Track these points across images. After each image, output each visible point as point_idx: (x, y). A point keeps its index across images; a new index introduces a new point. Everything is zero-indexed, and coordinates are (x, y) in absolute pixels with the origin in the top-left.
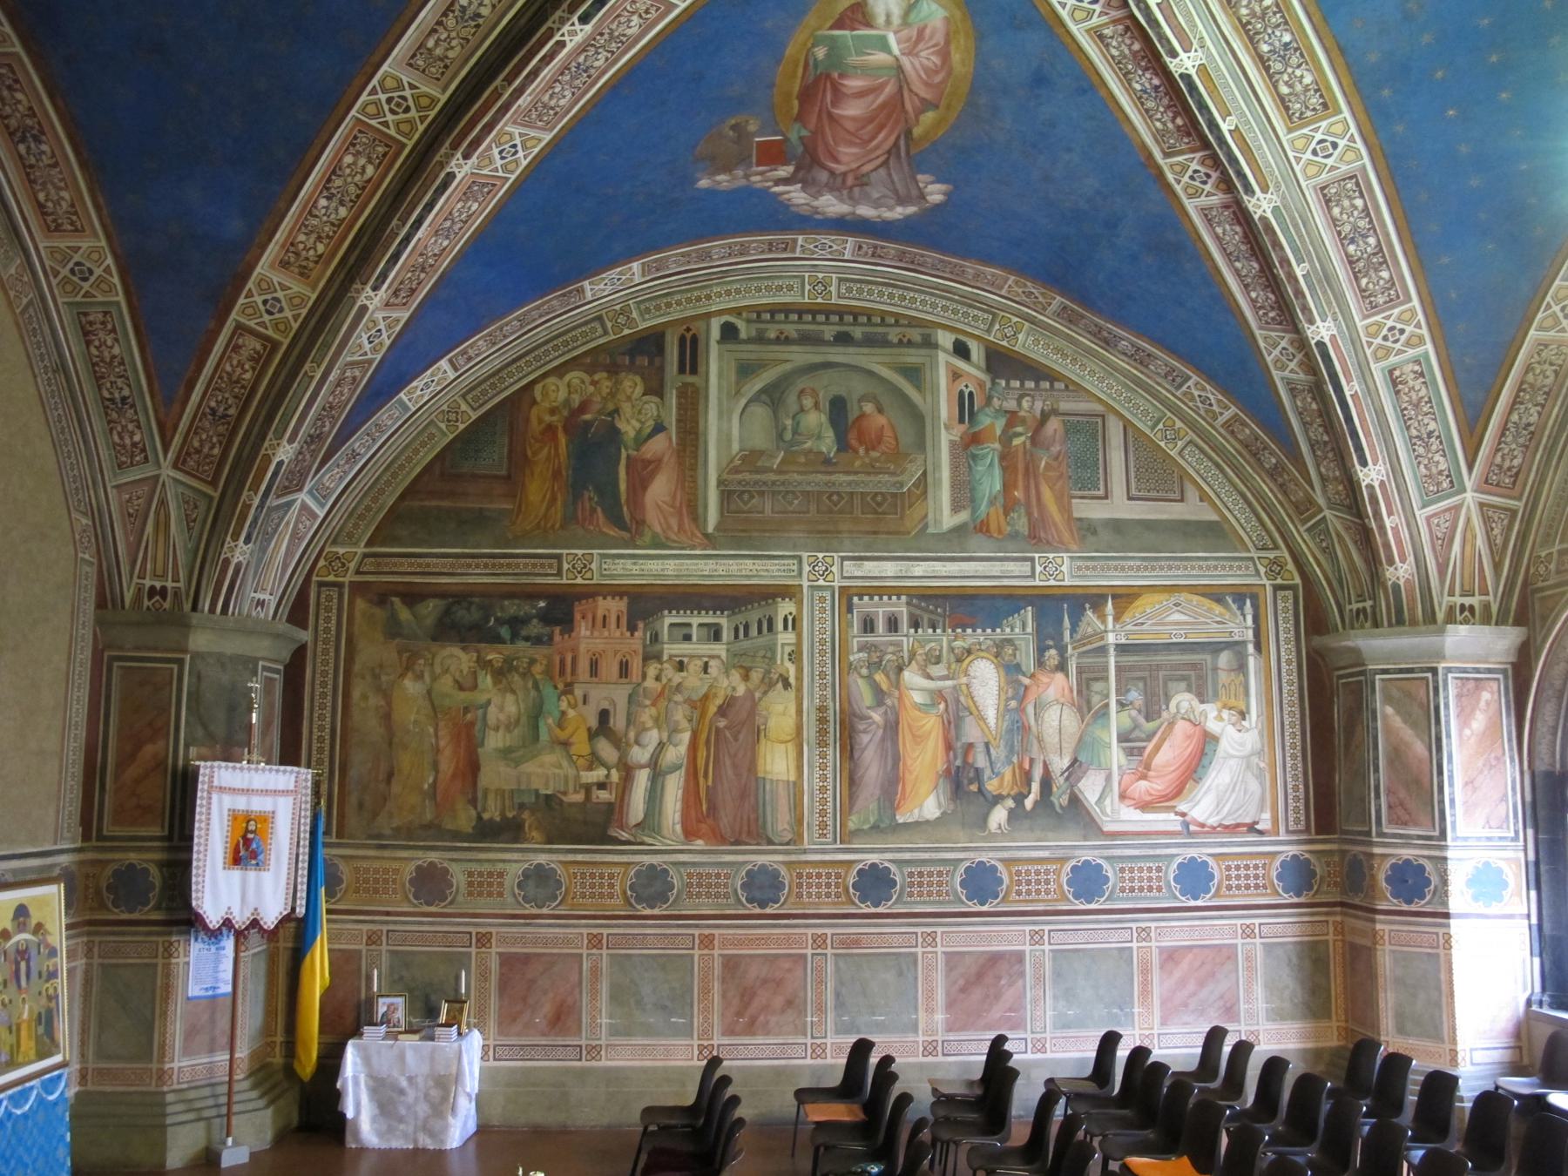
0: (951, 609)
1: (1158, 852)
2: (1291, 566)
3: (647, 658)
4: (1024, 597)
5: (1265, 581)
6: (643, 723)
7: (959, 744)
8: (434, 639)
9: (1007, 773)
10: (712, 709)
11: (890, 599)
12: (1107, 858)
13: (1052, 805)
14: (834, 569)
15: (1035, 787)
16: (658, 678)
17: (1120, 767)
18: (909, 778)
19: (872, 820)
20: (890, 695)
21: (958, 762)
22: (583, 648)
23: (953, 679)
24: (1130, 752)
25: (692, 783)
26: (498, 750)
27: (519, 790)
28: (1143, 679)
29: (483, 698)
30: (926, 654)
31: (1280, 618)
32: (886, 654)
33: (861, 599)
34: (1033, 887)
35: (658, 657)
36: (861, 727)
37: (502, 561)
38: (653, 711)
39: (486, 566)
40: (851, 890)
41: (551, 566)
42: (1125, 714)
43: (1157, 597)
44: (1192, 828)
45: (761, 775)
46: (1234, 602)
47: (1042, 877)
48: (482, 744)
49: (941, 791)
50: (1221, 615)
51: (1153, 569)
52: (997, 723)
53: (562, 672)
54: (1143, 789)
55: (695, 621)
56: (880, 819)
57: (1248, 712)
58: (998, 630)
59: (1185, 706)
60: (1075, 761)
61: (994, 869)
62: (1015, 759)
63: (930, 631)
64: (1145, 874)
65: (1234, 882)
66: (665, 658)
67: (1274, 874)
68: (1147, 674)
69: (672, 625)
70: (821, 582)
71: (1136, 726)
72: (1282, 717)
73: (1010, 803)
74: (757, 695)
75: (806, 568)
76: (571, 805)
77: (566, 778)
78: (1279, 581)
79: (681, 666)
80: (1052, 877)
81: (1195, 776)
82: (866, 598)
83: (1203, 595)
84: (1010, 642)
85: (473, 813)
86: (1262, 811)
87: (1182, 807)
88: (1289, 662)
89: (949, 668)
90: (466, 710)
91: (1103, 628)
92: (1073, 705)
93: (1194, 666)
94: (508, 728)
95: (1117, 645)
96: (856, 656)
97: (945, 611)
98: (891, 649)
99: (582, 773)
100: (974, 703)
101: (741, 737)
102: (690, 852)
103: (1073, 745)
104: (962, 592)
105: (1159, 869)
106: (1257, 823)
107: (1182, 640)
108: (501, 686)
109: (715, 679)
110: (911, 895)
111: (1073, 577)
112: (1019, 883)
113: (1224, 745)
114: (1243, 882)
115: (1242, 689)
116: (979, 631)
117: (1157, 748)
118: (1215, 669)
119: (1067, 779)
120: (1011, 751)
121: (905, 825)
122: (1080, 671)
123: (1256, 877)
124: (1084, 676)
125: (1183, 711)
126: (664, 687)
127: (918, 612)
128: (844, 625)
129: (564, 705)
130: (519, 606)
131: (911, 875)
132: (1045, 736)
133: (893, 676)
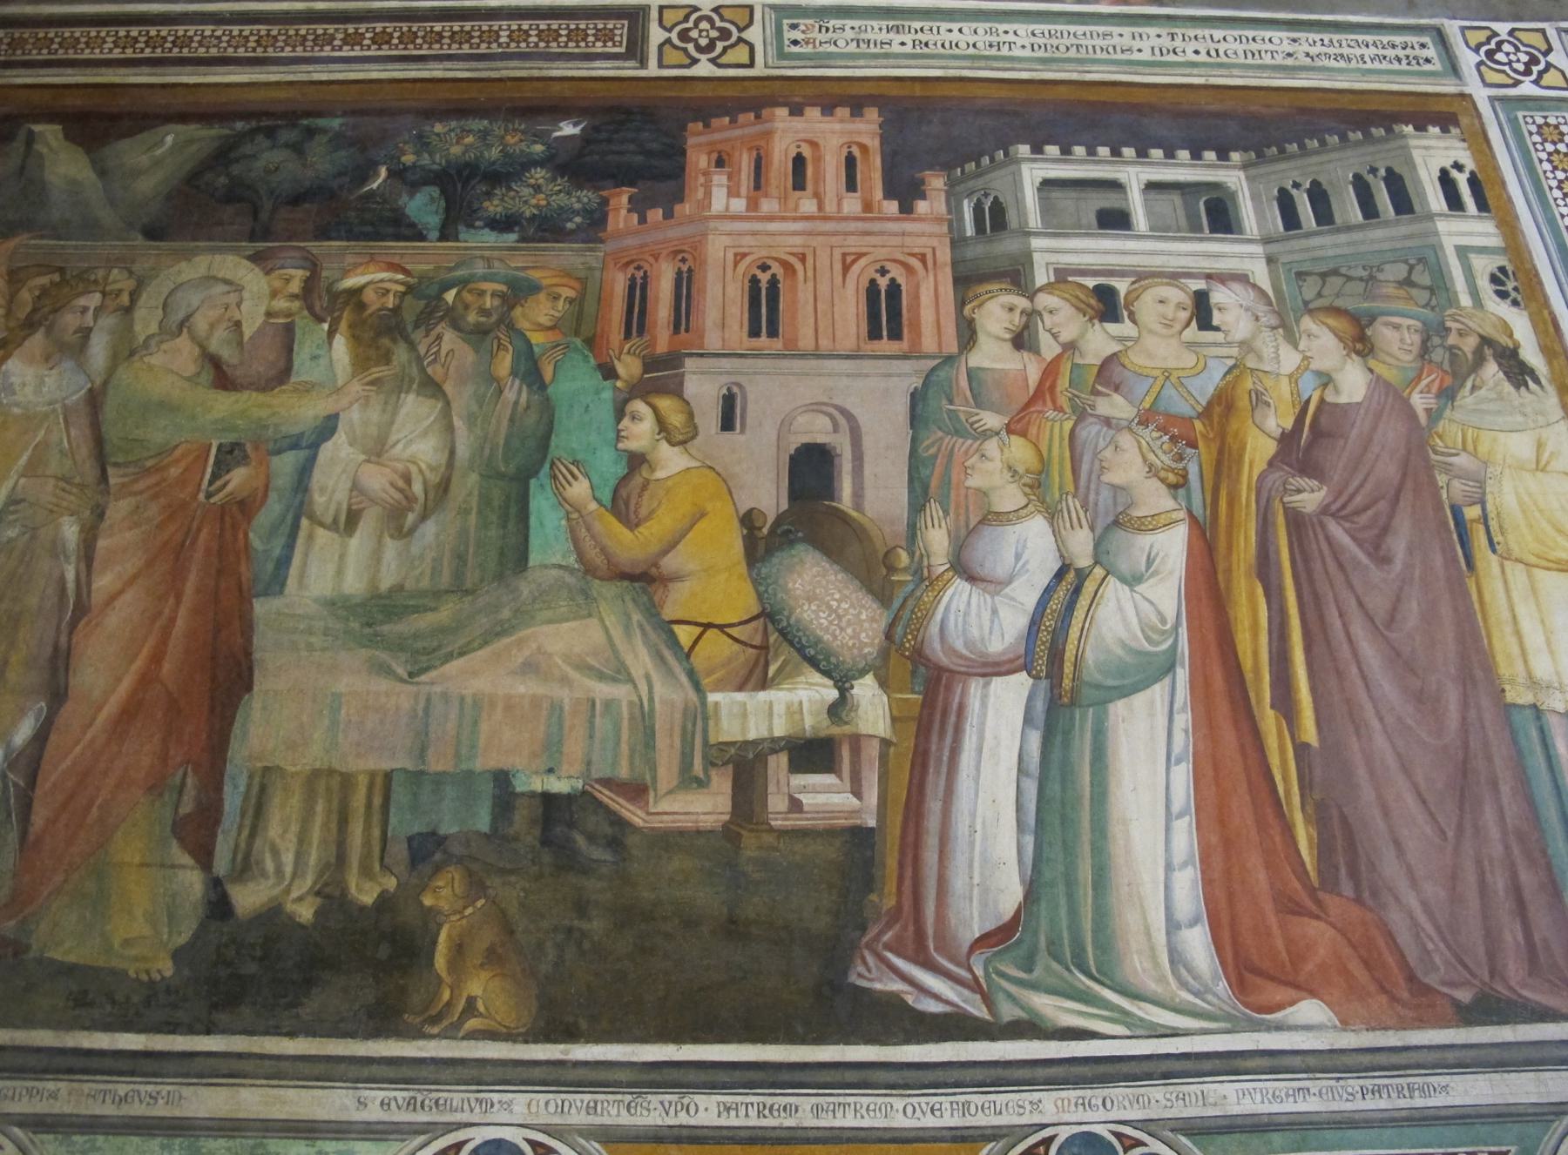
3: (967, 280)
6: (983, 494)
8: (153, 233)
10: (1259, 448)
16: (1022, 340)
22: (717, 248)
25: (1229, 736)
26: (337, 605)
27: (417, 777)
29: (306, 412)
35: (1016, 275)
37: (438, 27)
38: (1019, 450)
39: (381, 39)
41: (607, 36)
45: (1517, 695)
48: (277, 583)
53: (637, 318)
55: (1134, 175)
66: (1041, 277)
69: (1047, 184)
74: (1419, 402)
75: (1468, 59)
76: (668, 841)
77: (644, 723)
79: (1106, 305)
85: (192, 882)
90: (231, 455)
94: (397, 521)
99: (713, 697)
101: (1398, 545)
102: (1274, 1063)
108: (377, 372)
109: (1246, 346)
126: (1050, 371)
129: (640, 431)
130: (484, 135)
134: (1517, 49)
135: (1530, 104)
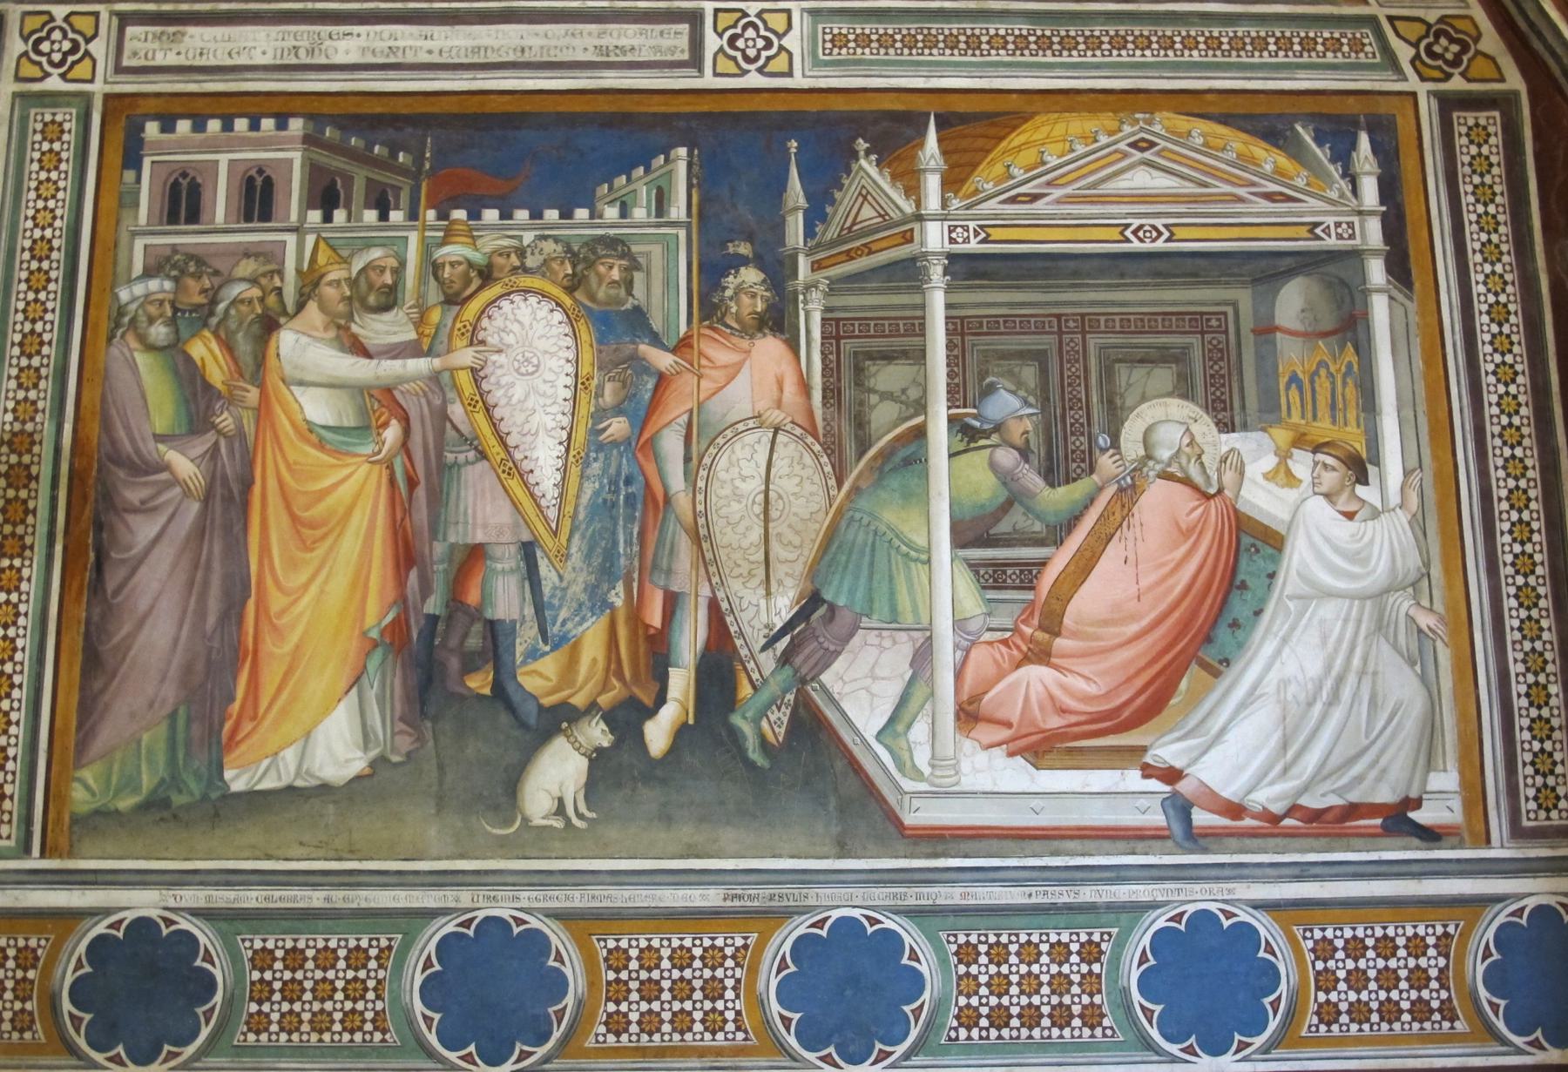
0: (439, 153)
1: (1088, 894)
2: (1491, 41)
4: (666, 120)
5: (1413, 83)
7: (439, 549)
9: (592, 638)
11: (255, 126)
12: (914, 913)
13: (735, 735)
14: (98, 48)
15: (680, 682)
17: (959, 624)
18: (276, 653)
19: (147, 782)
20: (231, 400)
21: (433, 605)
23: (429, 353)
24: (992, 577)
28: (1040, 357)
30: (353, 283)
31: (1465, 188)
32: (230, 280)
33: (168, 126)
34: (665, 1006)
36: (134, 495)
40: (67, 1006)
42: (978, 459)
43: (1078, 124)
44: (1201, 818)
46: (1319, 141)
47: (697, 974)
49: (372, 694)
50: (1279, 175)
51: (1068, 44)
52: (563, 485)
54: (1036, 691)
56: (174, 780)
57: (1376, 461)
58: (582, 214)
59: (1169, 440)
60: (812, 602)
61: (537, 941)
62: (618, 598)
63: (371, 216)
64: (1045, 968)
65: (1344, 996)
67: (1478, 970)
68: (1047, 342)
70: (54, 83)
71: (1014, 498)
72: (1484, 474)
73: (597, 733)
78: (1457, 84)
80: (729, 973)
81: (1209, 654)
82: (184, 126)
83: (1225, 119)
84: (616, 245)
86: (1429, 766)
87: (1167, 752)
88: (1499, 314)
89: (420, 322)
91: (908, 207)
92: (815, 436)
93: (1198, 322)
95: (952, 257)
96: (139, 289)
97: (419, 160)
98: (247, 268)
100: (494, 425)
103: (809, 552)
104: (472, 106)
105: (1091, 953)
106: (1417, 804)
107: (1160, 245)
110: (258, 1024)
111: (817, 63)
112: (618, 992)
113: (1298, 554)
114: (1373, 995)
115: (1351, 392)
116: (522, 215)
117: (1084, 566)
118: (1266, 330)
119: (785, 659)
120: (607, 571)
121: (256, 801)
122: (834, 330)
123: (1419, 979)
124: (848, 346)
125: (1164, 454)
127: (337, 163)
128: (108, 202)
131: (263, 959)
132: (718, 526)
133: (244, 346)
134: (65, 36)
135: (47, 100)
